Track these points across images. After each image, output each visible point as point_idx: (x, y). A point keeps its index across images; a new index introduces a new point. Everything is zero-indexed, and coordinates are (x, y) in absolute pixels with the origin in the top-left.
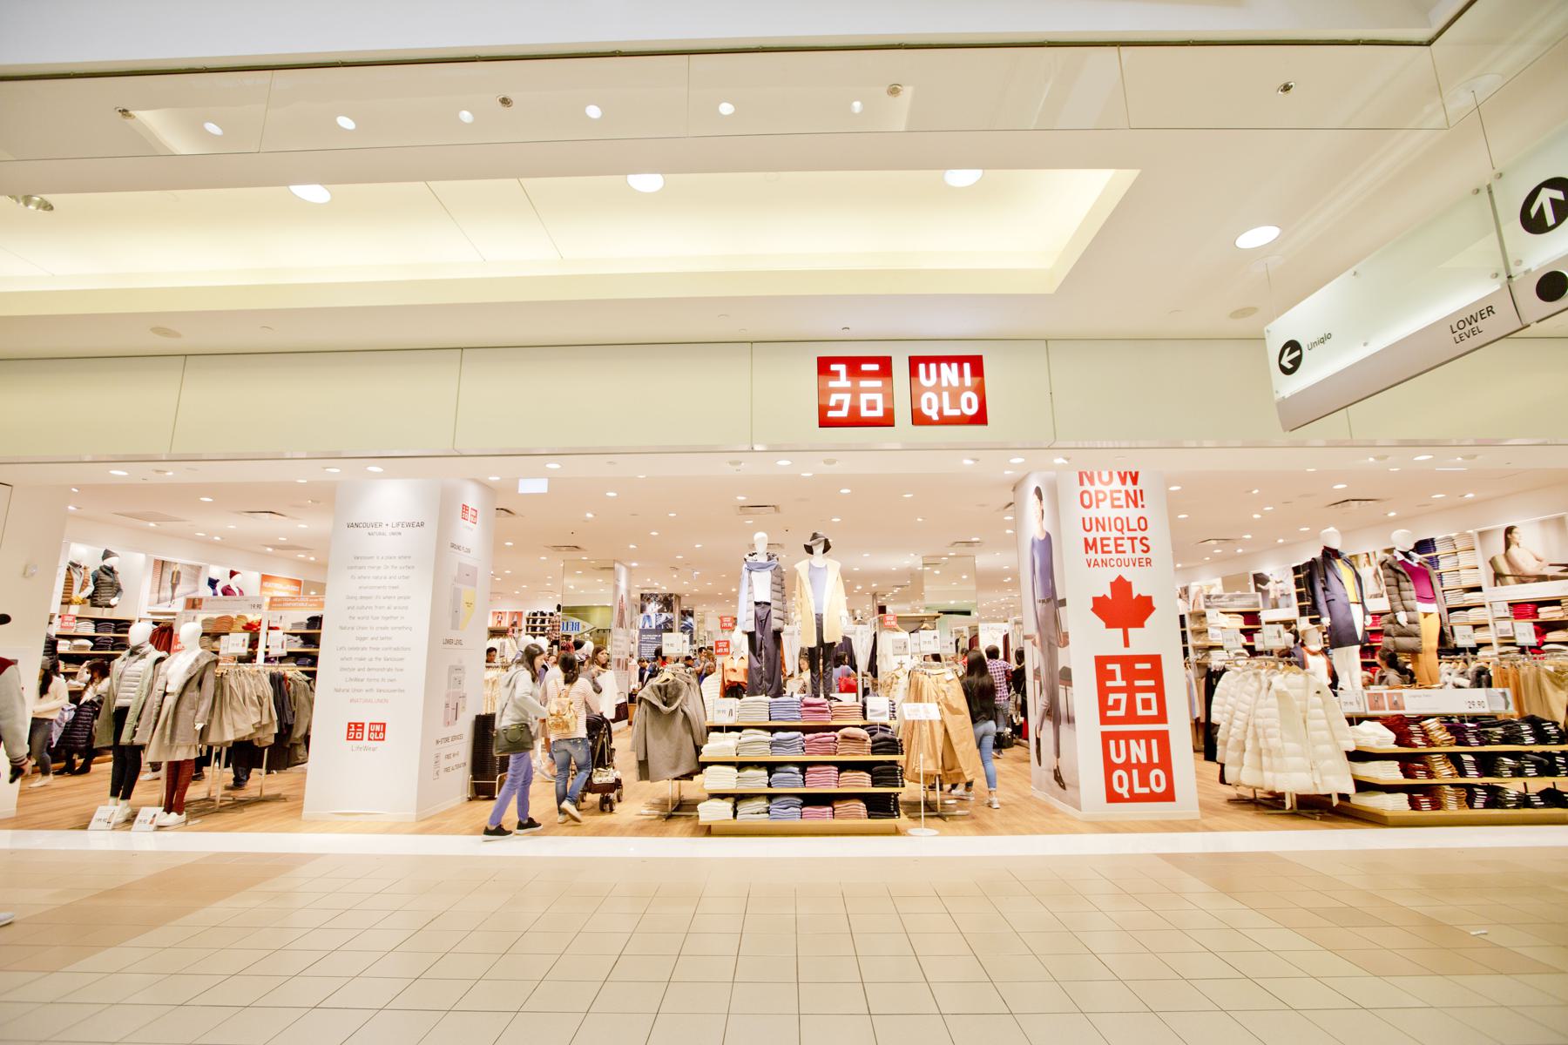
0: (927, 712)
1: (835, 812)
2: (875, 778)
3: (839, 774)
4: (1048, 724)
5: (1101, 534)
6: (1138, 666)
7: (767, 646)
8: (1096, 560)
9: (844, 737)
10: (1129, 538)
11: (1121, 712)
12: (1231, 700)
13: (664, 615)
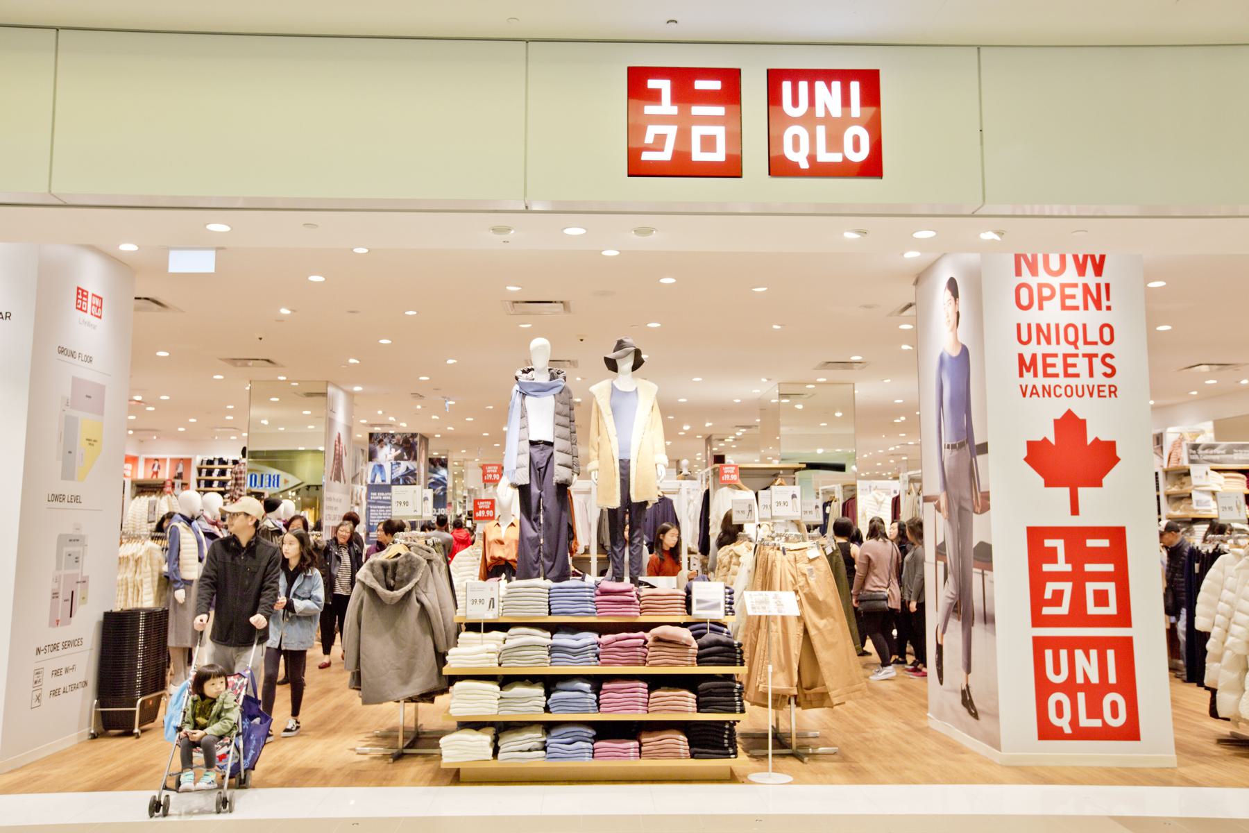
0: (779, 604)
1: (643, 748)
2: (701, 699)
3: (649, 693)
4: (955, 626)
5: (1044, 348)
6: (1091, 543)
7: (547, 506)
8: (1034, 387)
9: (658, 640)
10: (1084, 355)
11: (1064, 610)
12: (1227, 595)
13: (404, 465)
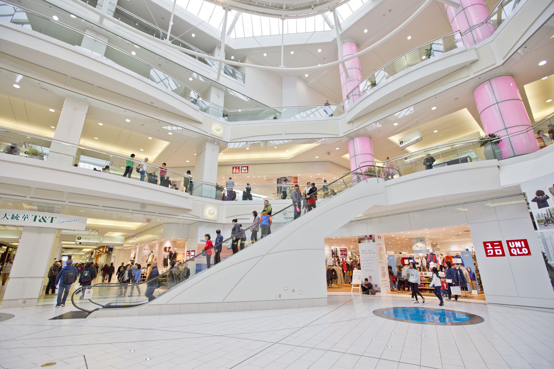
6: (495, 244)
